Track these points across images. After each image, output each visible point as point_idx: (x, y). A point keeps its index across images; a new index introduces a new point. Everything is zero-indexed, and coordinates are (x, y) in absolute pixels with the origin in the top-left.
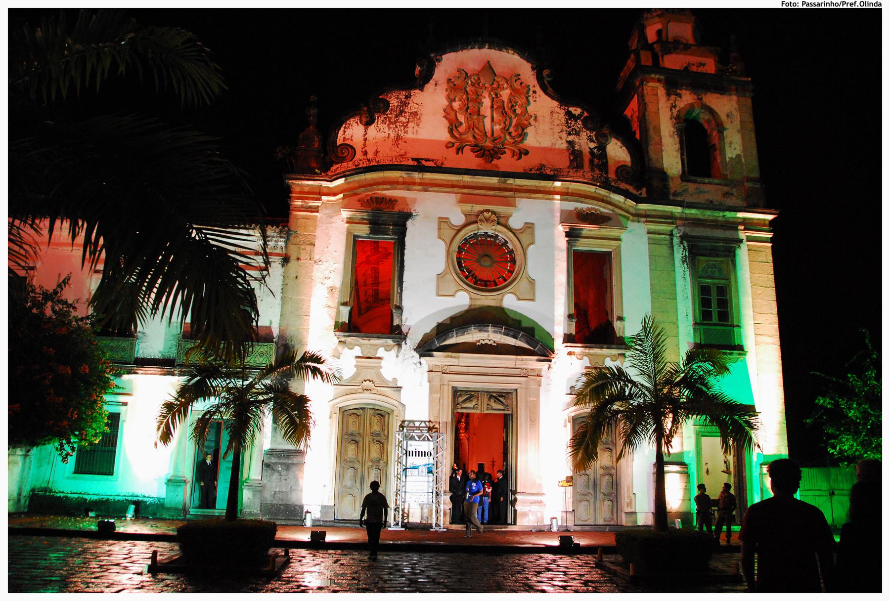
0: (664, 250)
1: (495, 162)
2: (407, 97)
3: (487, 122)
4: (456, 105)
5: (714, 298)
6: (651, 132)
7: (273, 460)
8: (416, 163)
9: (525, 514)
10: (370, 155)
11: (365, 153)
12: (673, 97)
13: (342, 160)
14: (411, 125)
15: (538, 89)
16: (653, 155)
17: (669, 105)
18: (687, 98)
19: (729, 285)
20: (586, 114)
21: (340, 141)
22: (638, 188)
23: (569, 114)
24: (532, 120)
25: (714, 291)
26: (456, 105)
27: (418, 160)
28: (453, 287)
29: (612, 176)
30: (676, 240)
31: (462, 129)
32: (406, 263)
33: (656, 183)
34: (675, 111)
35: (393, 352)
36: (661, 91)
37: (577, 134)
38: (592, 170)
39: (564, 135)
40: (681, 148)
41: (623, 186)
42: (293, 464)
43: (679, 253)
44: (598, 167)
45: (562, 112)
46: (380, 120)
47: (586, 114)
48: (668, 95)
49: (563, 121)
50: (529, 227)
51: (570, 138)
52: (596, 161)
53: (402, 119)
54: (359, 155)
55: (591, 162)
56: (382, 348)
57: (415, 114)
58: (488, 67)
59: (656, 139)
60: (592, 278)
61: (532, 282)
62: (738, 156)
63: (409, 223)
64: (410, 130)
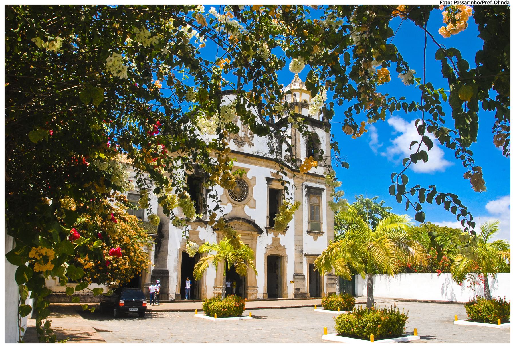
1: (242, 147)
7: (156, 275)
9: (251, 295)
29: (283, 159)
30: (304, 187)
35: (203, 228)
41: (287, 163)
42: (165, 277)
43: (305, 192)
50: (254, 178)
61: (255, 201)
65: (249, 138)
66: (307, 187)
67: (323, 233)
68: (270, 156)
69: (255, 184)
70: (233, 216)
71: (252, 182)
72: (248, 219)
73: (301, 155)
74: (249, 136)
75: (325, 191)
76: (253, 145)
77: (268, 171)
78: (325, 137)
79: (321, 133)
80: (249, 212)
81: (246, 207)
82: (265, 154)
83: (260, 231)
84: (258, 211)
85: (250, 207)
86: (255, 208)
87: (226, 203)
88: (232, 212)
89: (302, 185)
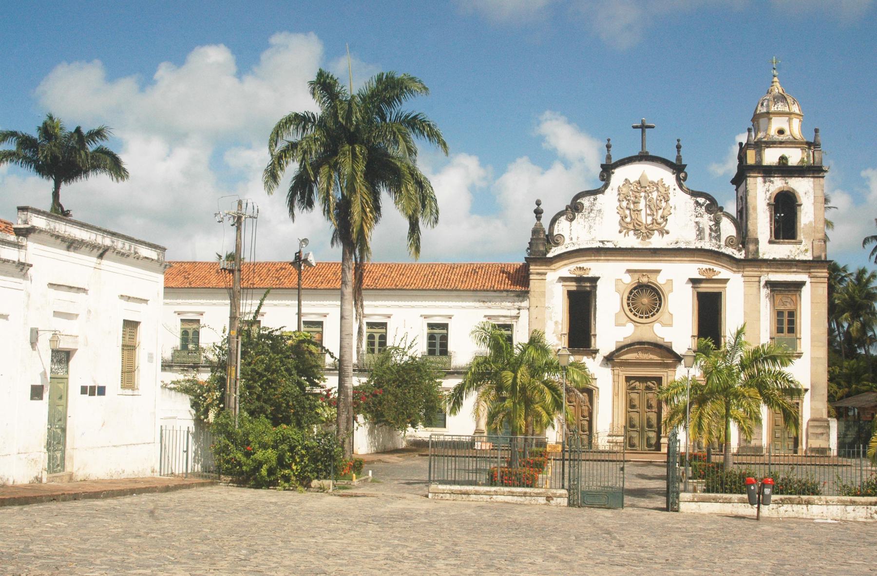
0: (754, 290)
2: (595, 200)
3: (643, 213)
4: (624, 204)
5: (786, 319)
6: (751, 211)
8: (601, 245)
10: (574, 240)
11: (571, 239)
12: (768, 184)
13: (557, 244)
14: (598, 218)
15: (677, 187)
16: (750, 227)
17: (765, 190)
18: (778, 184)
19: (796, 310)
20: (708, 202)
21: (555, 233)
22: (740, 250)
23: (697, 203)
24: (672, 211)
25: (786, 314)
26: (624, 204)
27: (602, 242)
28: (626, 318)
29: (723, 243)
31: (628, 220)
32: (598, 307)
33: (751, 247)
34: (768, 194)
36: (760, 180)
37: (701, 216)
38: (711, 240)
39: (693, 218)
40: (771, 221)
41: (729, 251)
43: (765, 292)
44: (715, 238)
45: (693, 202)
46: (578, 216)
47: (708, 202)
48: (765, 182)
49: (693, 208)
51: (697, 220)
52: (713, 234)
53: (591, 215)
54: (567, 241)
55: (710, 235)
56: (586, 360)
57: (600, 211)
58: (643, 176)
59: (754, 215)
60: (709, 310)
62: (811, 223)
63: (599, 283)
64: (597, 222)
65: (660, 224)
66: (769, 284)
67: (799, 356)
68: (699, 245)
69: (671, 291)
70: (636, 340)
71: (665, 289)
72: (660, 342)
73: (759, 231)
74: (660, 221)
75: (808, 285)
76: (667, 233)
77: (694, 269)
78: (811, 191)
79: (802, 186)
80: (660, 332)
81: (657, 327)
82: (689, 243)
83: (678, 359)
84: (678, 327)
85: (664, 325)
86: (671, 325)
87: (624, 322)
88: (634, 333)
89: (759, 282)
